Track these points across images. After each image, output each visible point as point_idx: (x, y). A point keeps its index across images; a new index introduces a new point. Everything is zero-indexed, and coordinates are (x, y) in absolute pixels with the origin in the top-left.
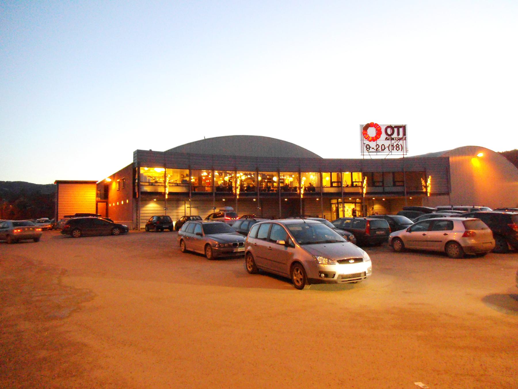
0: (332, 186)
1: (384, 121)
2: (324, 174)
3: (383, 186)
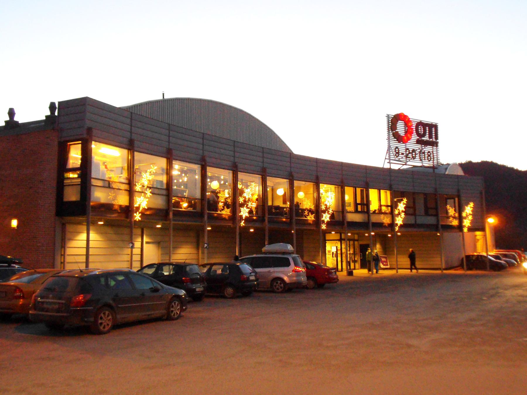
0: (356, 211)
1: (416, 115)
2: (323, 188)
3: (437, 215)
